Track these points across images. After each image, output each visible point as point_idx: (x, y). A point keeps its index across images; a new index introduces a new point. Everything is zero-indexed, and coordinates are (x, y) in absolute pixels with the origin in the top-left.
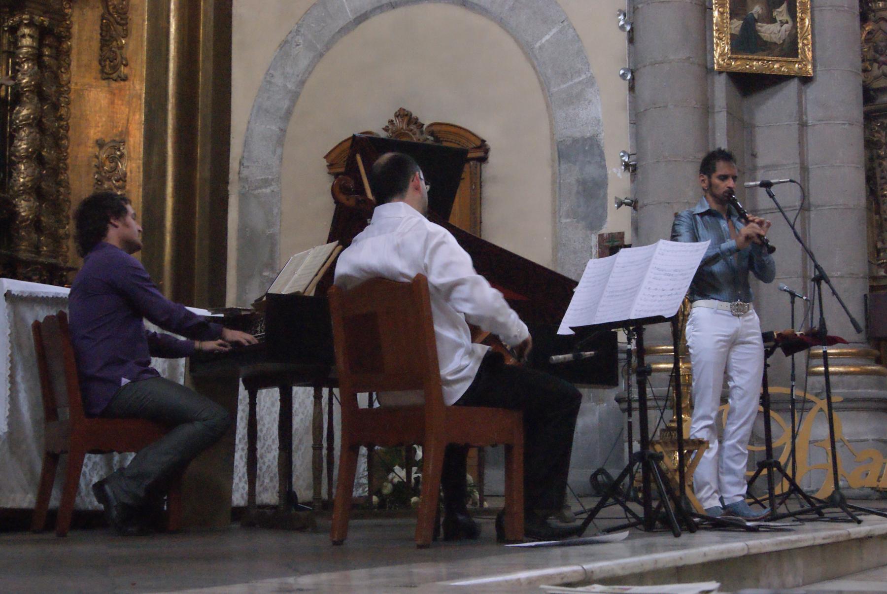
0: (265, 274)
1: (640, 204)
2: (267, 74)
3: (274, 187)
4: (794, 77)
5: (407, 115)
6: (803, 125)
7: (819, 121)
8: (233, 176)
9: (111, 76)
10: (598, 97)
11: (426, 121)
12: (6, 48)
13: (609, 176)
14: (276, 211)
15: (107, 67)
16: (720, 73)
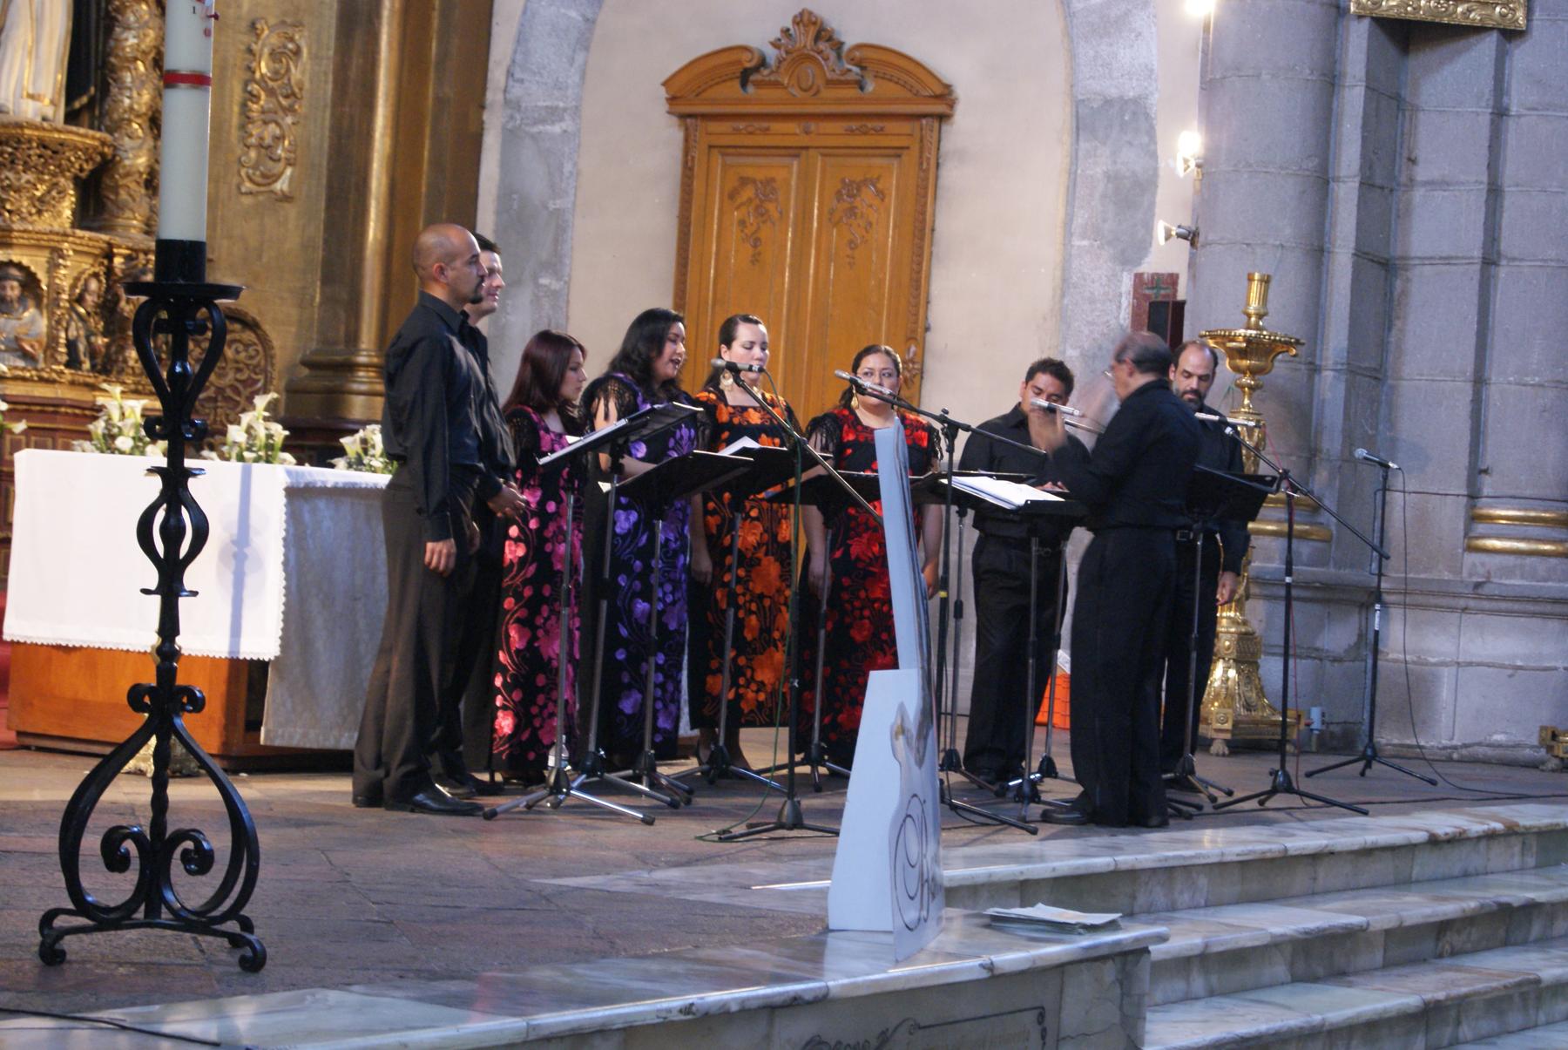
0: (544, 281)
1: (1201, 239)
3: (567, 124)
4: (1492, 29)
5: (815, 23)
6: (1500, 114)
7: (1529, 109)
8: (493, 96)
10: (1154, 29)
11: (850, 39)
13: (1161, 173)
14: (568, 167)
16: (1360, 17)
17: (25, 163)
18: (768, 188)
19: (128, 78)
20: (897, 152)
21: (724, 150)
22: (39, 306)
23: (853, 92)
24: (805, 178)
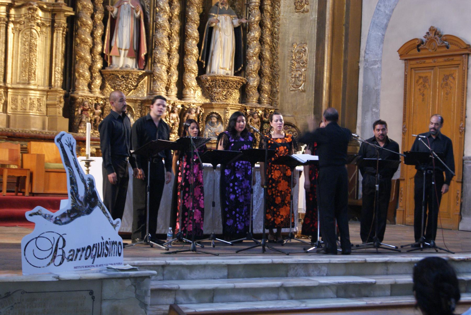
0: (374, 110)
2: (377, 5)
3: (378, 65)
5: (434, 30)
8: (362, 59)
9: (300, 11)
12: (246, 3)
14: (379, 77)
15: (298, 6)
17: (219, 86)
18: (426, 79)
19: (251, 61)
20: (457, 66)
21: (415, 69)
22: (222, 124)
23: (446, 49)
24: (435, 75)
